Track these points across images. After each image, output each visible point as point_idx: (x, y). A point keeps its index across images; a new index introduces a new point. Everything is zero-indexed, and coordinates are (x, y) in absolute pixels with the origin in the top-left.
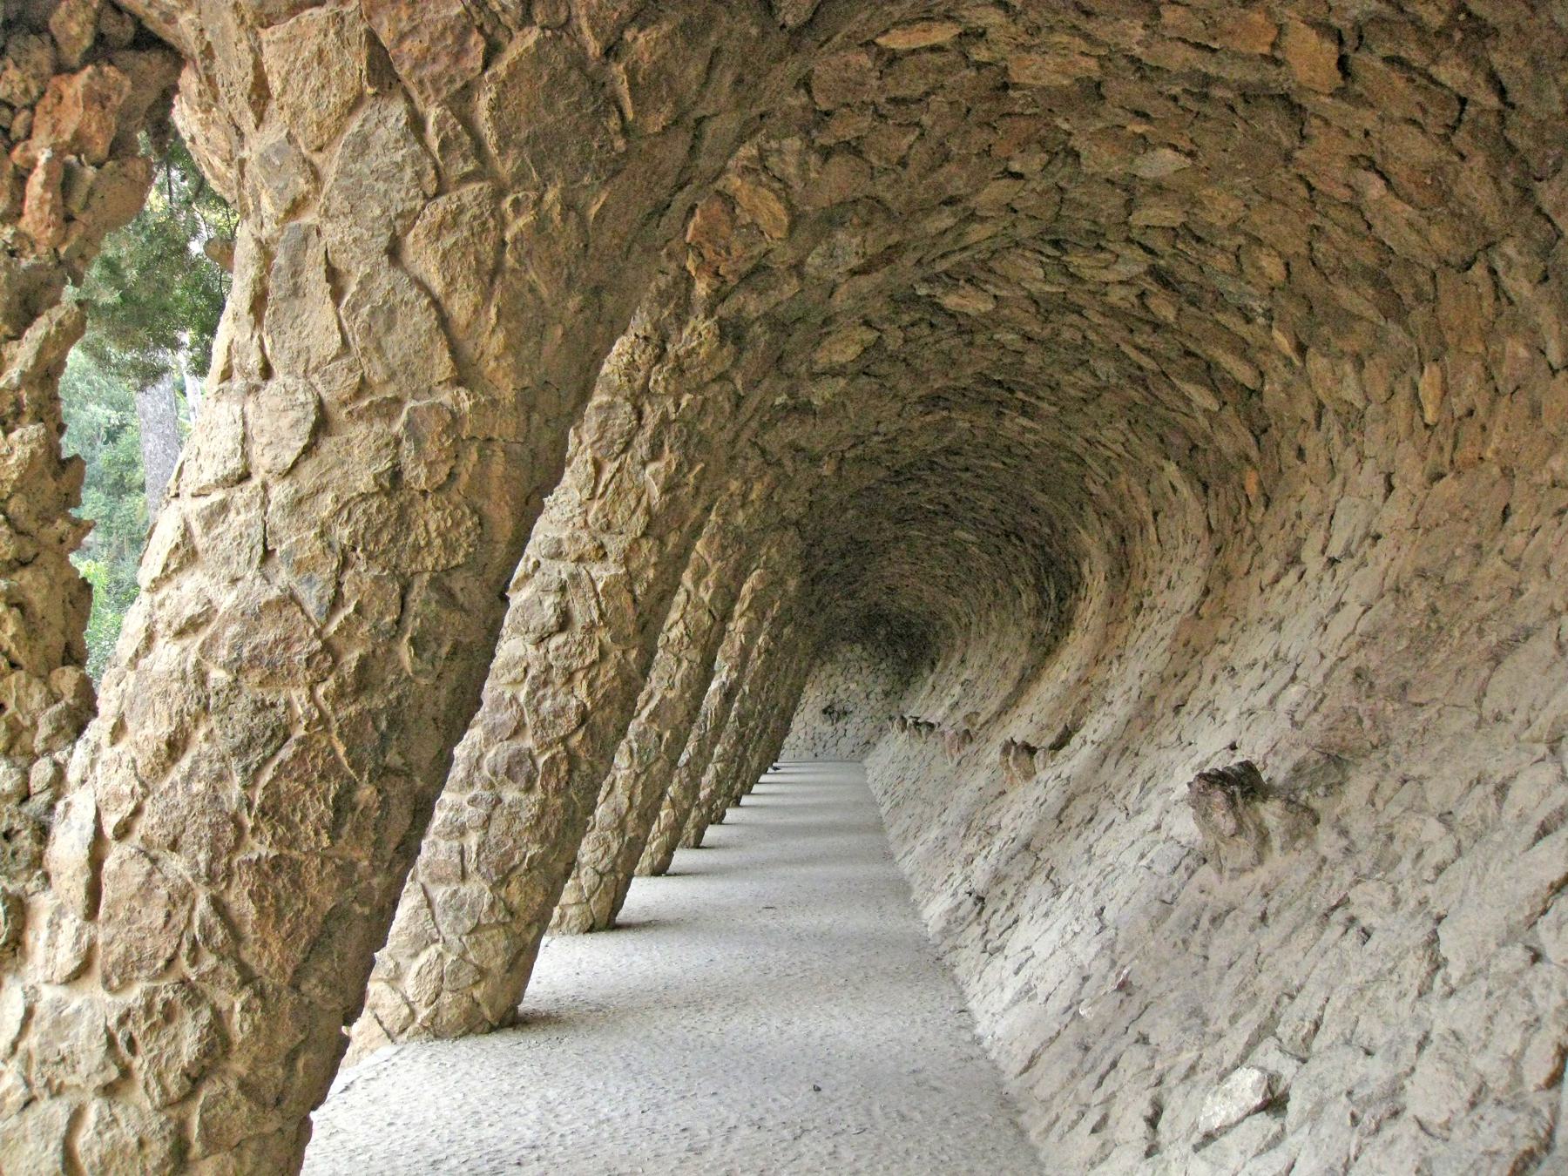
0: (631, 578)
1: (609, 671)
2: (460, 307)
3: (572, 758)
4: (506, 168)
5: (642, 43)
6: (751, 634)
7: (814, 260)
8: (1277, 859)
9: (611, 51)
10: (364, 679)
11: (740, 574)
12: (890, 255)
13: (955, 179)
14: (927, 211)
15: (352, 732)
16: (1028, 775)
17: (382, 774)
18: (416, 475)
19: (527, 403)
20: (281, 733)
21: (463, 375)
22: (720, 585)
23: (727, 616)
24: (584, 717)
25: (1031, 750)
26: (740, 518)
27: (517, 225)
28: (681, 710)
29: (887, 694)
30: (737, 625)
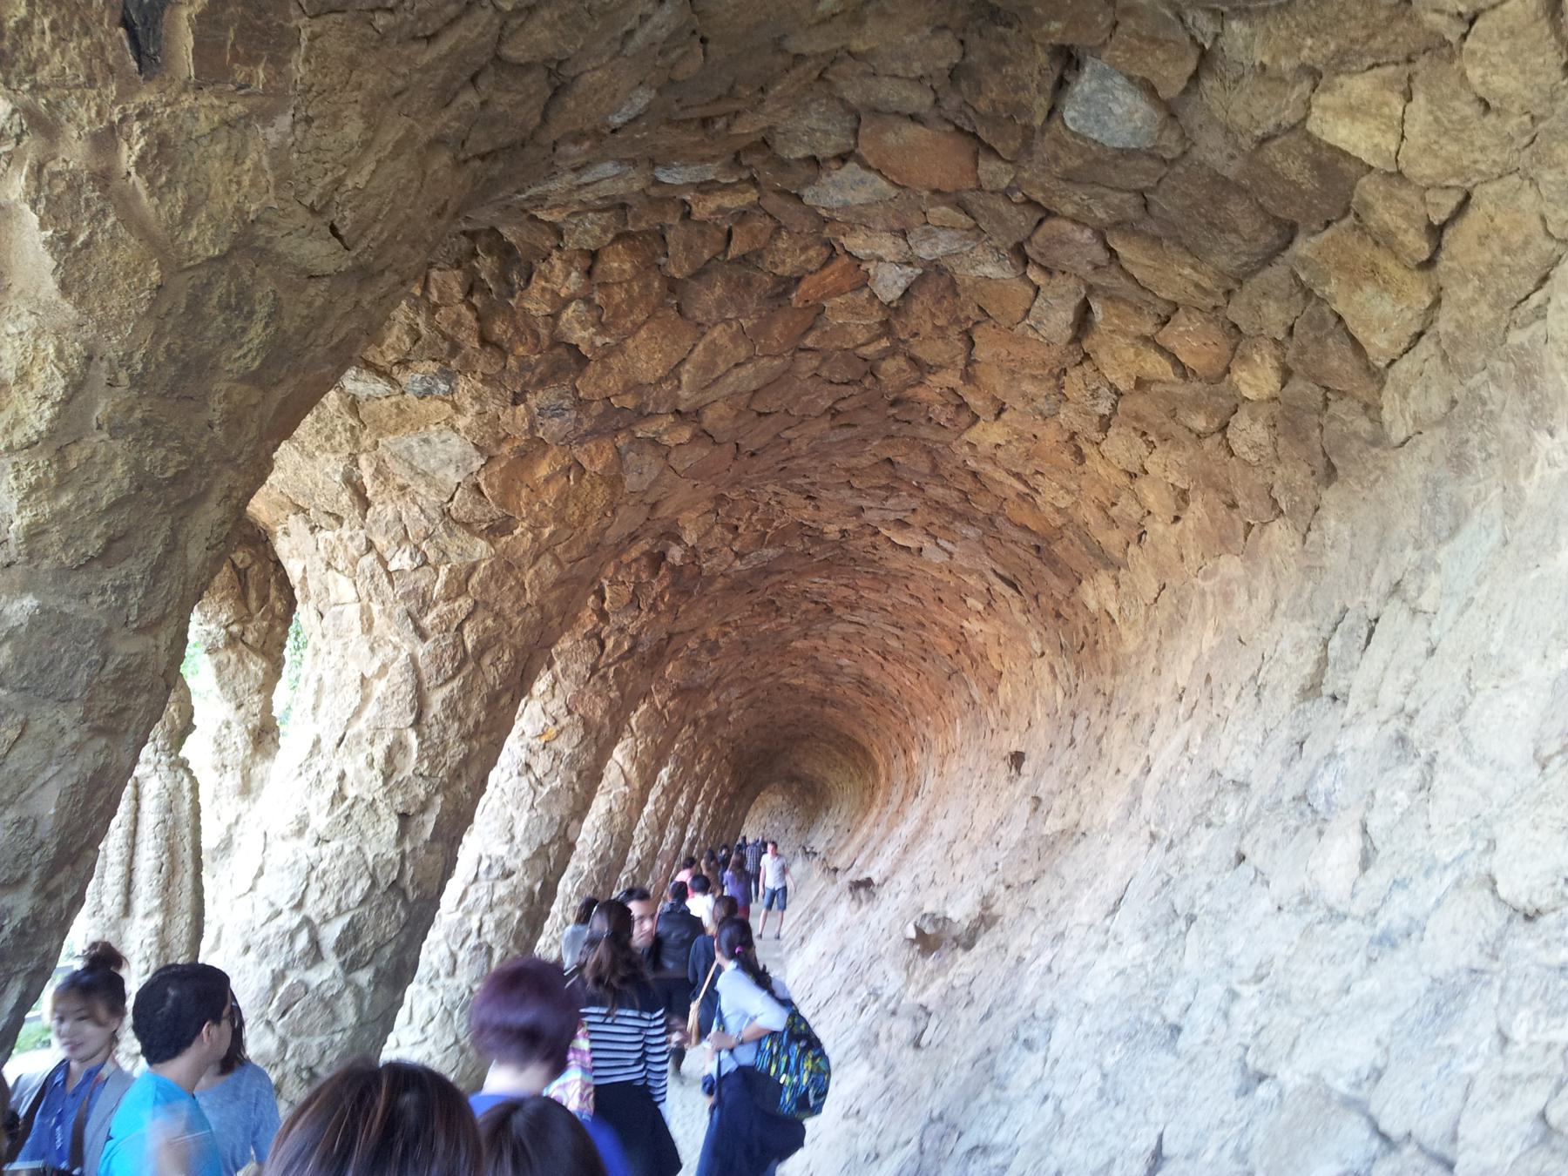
0: (656, 811)
1: (648, 845)
2: (627, 767)
3: (634, 877)
4: (638, 734)
5: (671, 704)
6: (704, 812)
7: (723, 697)
8: (864, 908)
9: (664, 706)
10: (602, 859)
11: (697, 793)
12: (751, 691)
13: (771, 669)
14: (763, 678)
15: (598, 874)
16: (834, 882)
17: (604, 884)
18: (616, 809)
19: (642, 788)
20: (581, 874)
21: (627, 782)
22: (689, 798)
23: (692, 811)
24: (639, 862)
25: (836, 870)
26: (697, 768)
27: (641, 747)
28: (671, 854)
29: (799, 829)
30: (698, 808)
